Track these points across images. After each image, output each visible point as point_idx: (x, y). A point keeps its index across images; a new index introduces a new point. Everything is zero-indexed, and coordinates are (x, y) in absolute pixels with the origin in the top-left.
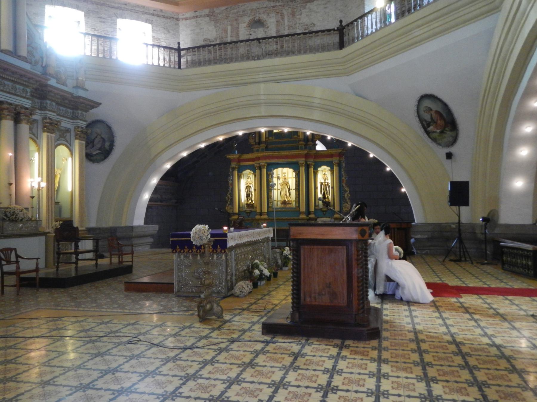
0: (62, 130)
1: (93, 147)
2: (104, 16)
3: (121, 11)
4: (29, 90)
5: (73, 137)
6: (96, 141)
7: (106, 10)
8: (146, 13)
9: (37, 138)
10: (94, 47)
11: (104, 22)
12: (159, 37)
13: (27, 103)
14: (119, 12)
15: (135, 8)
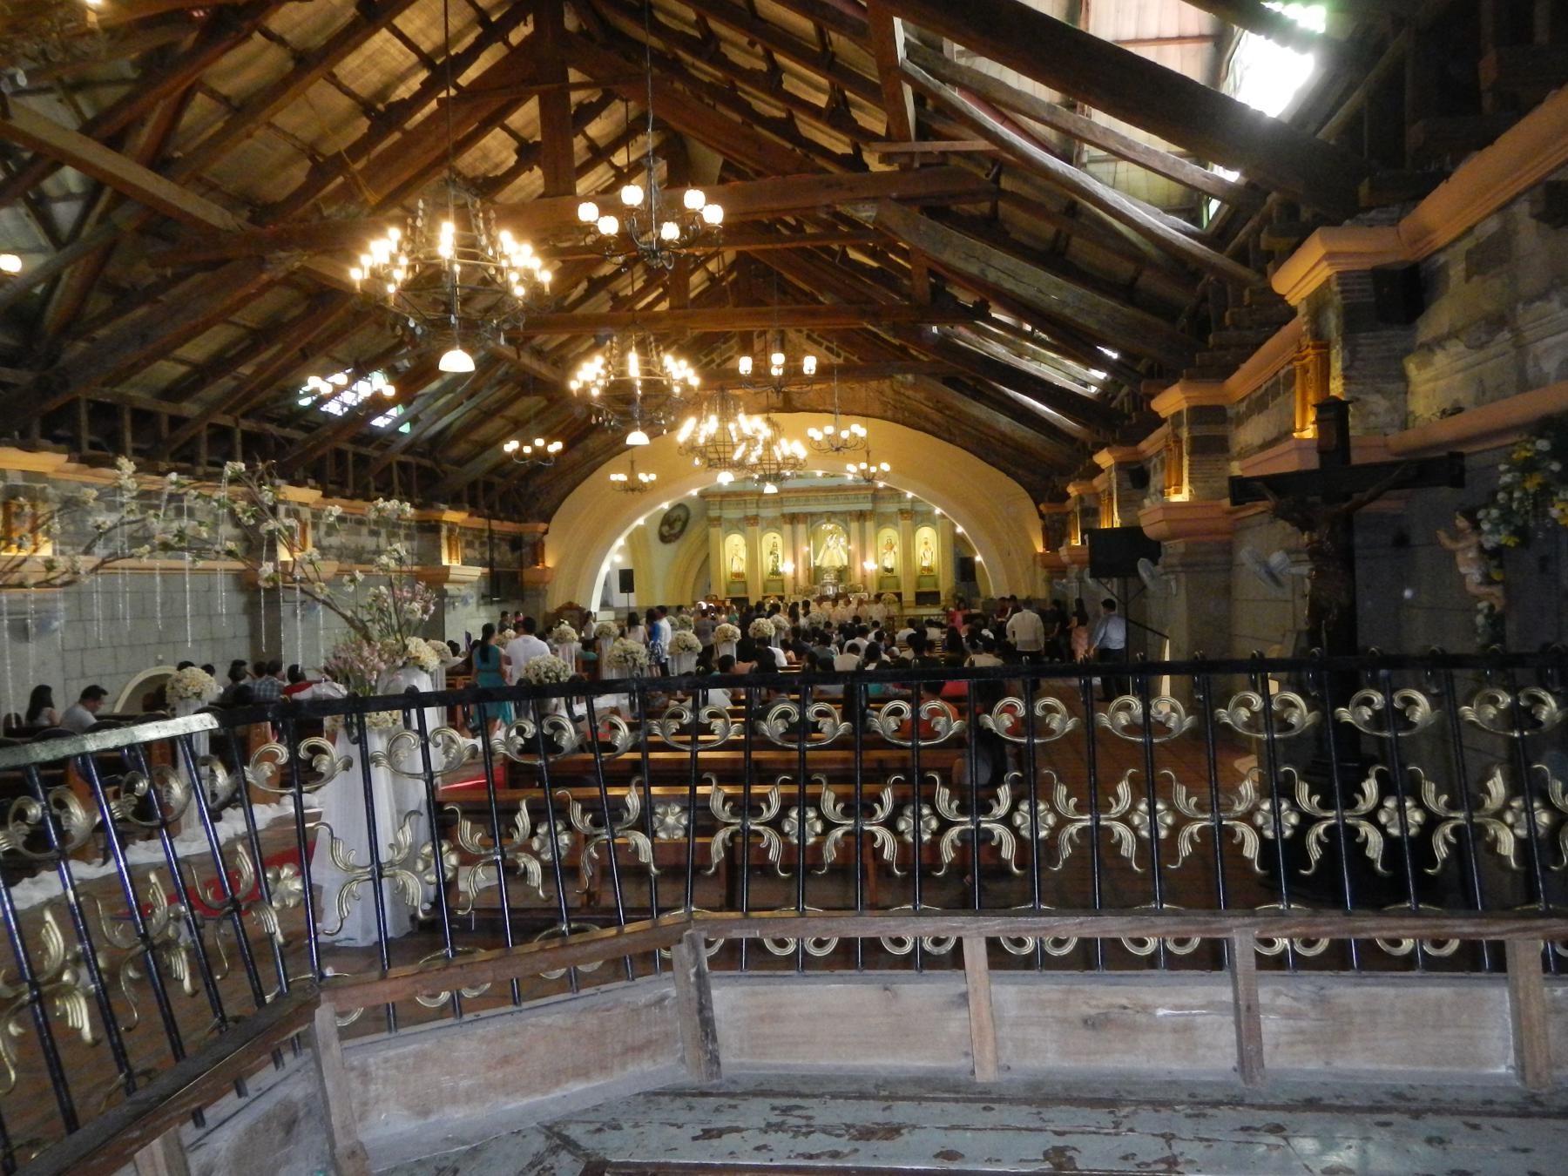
13: (867, 506)
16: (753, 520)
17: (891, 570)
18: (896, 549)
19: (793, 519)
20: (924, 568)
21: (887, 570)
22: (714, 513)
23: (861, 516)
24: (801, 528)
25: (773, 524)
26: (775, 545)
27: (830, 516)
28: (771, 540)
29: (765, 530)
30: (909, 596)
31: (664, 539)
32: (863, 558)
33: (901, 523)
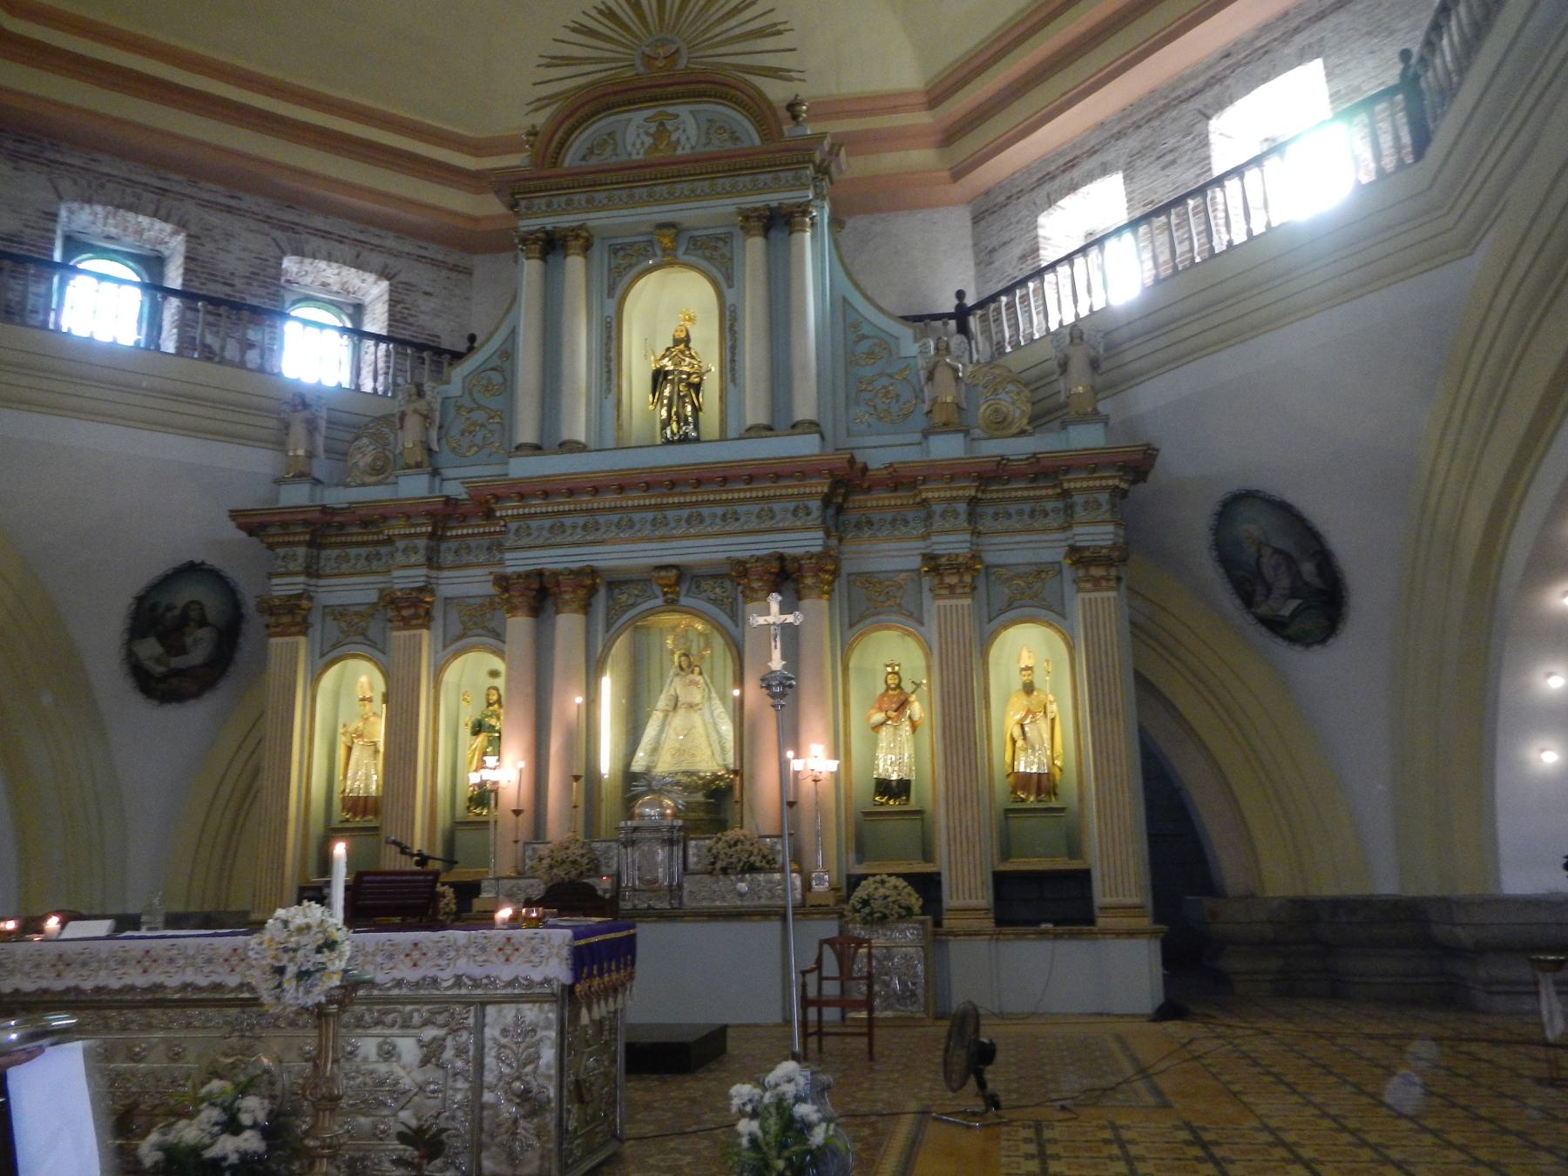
0: (1019, 576)
1: (1269, 590)
2: (1171, 142)
3: (1217, 88)
4: (815, 505)
5: (1069, 588)
6: (1268, 571)
7: (1174, 120)
8: (1297, 30)
9: (921, 623)
10: (1164, 256)
11: (1174, 162)
12: (1356, 83)
13: (805, 542)
14: (1209, 96)
15: (1258, 44)
16: (411, 609)
17: (901, 788)
18: (916, 709)
19: (541, 595)
20: (1024, 781)
21: (884, 787)
22: (285, 587)
23: (785, 577)
24: (568, 625)
25: (477, 626)
26: (494, 702)
27: (677, 582)
28: (470, 678)
29: (454, 645)
30: (966, 890)
31: (160, 686)
32: (790, 736)
33: (934, 607)
